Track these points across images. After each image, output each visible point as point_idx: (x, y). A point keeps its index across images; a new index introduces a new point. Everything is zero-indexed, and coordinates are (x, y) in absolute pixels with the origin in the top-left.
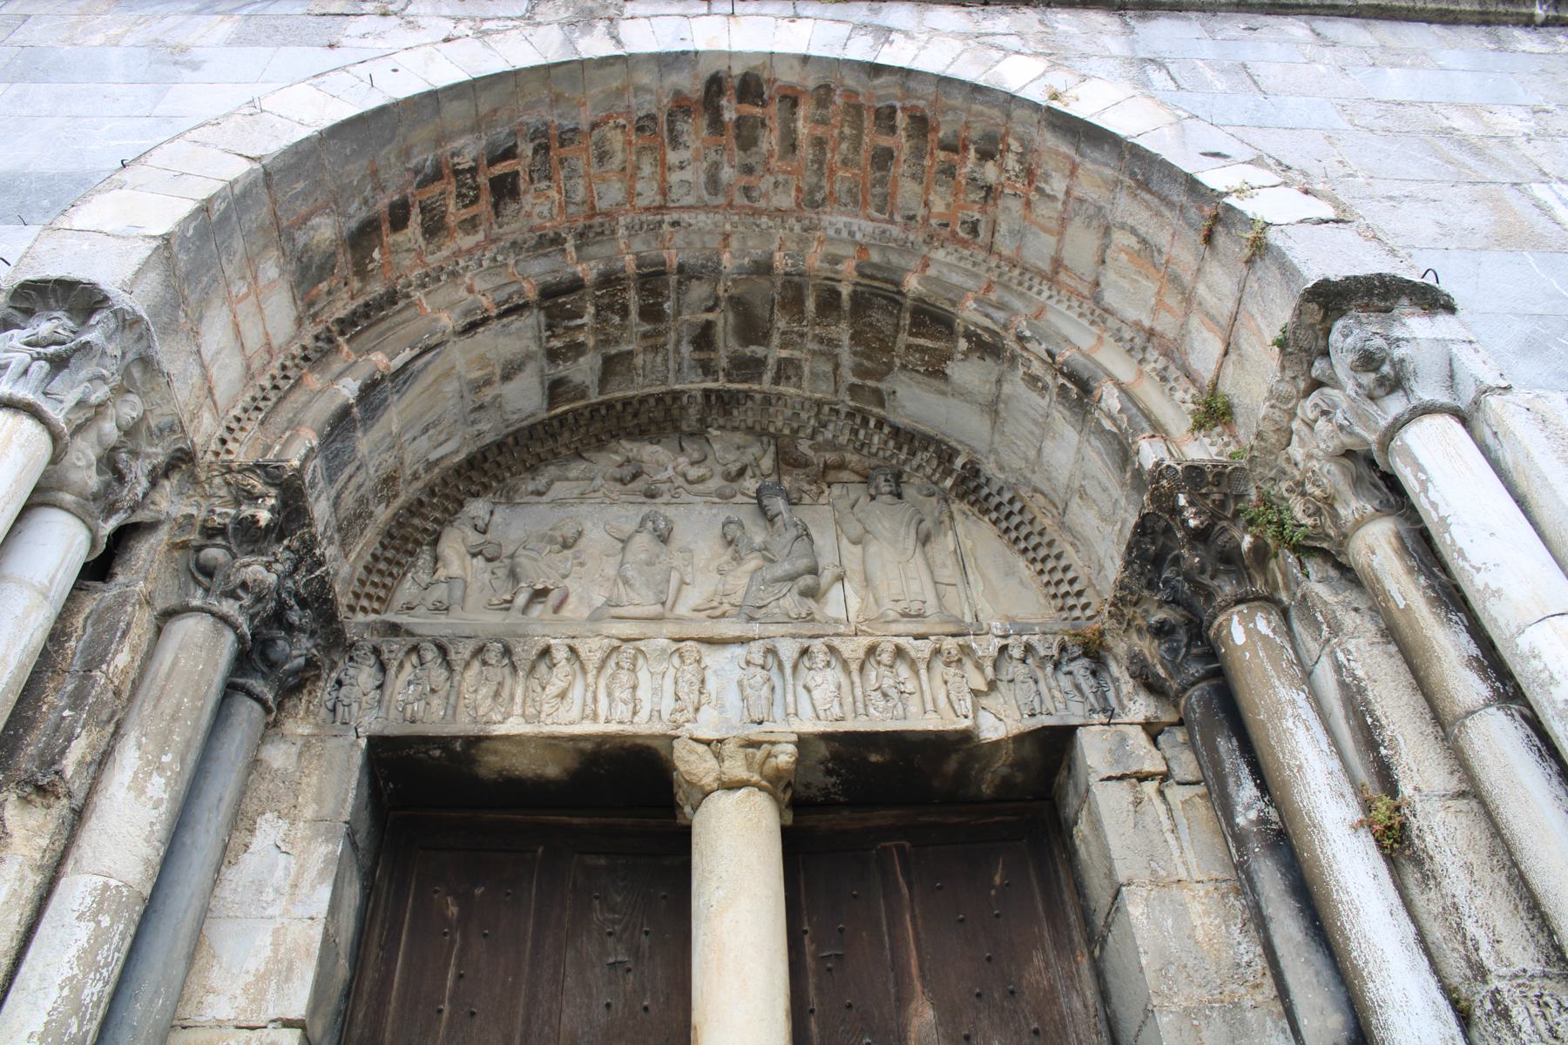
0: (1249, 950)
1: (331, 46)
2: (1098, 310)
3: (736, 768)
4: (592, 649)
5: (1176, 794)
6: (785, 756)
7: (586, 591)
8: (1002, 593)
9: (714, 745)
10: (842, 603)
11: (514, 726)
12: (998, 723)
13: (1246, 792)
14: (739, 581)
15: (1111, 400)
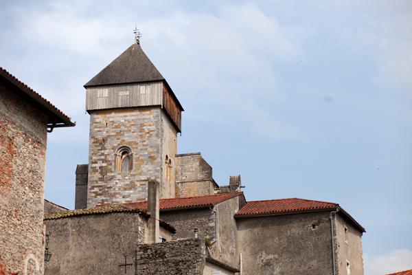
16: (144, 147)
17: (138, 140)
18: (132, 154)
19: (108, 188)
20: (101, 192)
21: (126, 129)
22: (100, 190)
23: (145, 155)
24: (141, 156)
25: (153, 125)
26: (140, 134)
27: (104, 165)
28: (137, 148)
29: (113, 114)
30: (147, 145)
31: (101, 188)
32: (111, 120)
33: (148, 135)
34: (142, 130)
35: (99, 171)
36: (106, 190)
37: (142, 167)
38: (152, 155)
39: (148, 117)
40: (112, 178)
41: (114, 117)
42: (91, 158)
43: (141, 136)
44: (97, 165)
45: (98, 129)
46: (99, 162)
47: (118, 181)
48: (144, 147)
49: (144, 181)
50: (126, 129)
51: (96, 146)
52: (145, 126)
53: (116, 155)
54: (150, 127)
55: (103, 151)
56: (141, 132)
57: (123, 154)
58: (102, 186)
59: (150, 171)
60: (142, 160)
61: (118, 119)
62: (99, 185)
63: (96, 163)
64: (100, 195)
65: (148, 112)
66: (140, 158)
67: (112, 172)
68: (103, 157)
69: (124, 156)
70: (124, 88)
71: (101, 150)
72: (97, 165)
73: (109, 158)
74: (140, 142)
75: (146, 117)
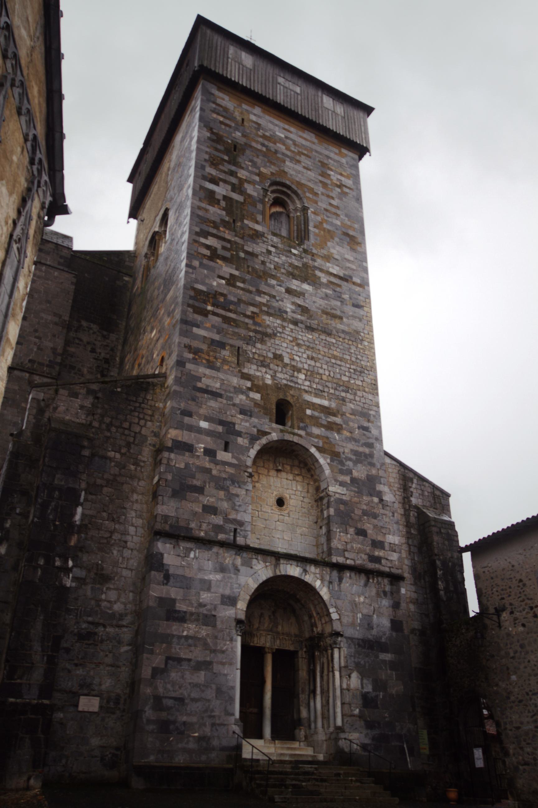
0: (307, 678)
1: (252, 568)
2: (315, 608)
3: (270, 651)
4: (258, 634)
5: (306, 660)
6: (274, 651)
7: (256, 626)
8: (294, 630)
9: (268, 648)
10: (280, 628)
11: (252, 644)
12: (292, 648)
13: (312, 665)
14: (271, 626)
15: (313, 621)
16: (333, 210)
17: (320, 189)
18: (305, 209)
19: (247, 253)
20: (228, 254)
21: (288, 153)
22: (224, 248)
23: (336, 225)
24: (327, 221)
25: (348, 177)
26: (320, 178)
27: (235, 196)
28: (316, 203)
29: (257, 110)
30: (337, 207)
31: (229, 246)
32: (253, 118)
33: (339, 190)
34: (324, 174)
35: (223, 204)
36: (242, 255)
37: (329, 244)
38: (351, 233)
39: (337, 158)
40: (256, 236)
41: (259, 117)
42: (203, 168)
43: (325, 185)
44: (221, 190)
45: (222, 119)
46: (221, 183)
47: (273, 249)
48: (333, 210)
49: (335, 276)
50: (288, 153)
51: (216, 149)
52: (332, 170)
53: (265, 191)
54: (343, 179)
55: (233, 168)
56: (322, 176)
57: (277, 202)
58: (229, 241)
59: (348, 261)
60: (329, 231)
61: (271, 126)
62: (221, 234)
63: (214, 181)
64: (224, 259)
65: (337, 151)
66: (325, 225)
67: (257, 222)
68: (233, 180)
69: (274, 210)
70: (288, 77)
71: (229, 162)
72: (221, 190)
73: (250, 189)
74: (323, 194)
75: (332, 155)
